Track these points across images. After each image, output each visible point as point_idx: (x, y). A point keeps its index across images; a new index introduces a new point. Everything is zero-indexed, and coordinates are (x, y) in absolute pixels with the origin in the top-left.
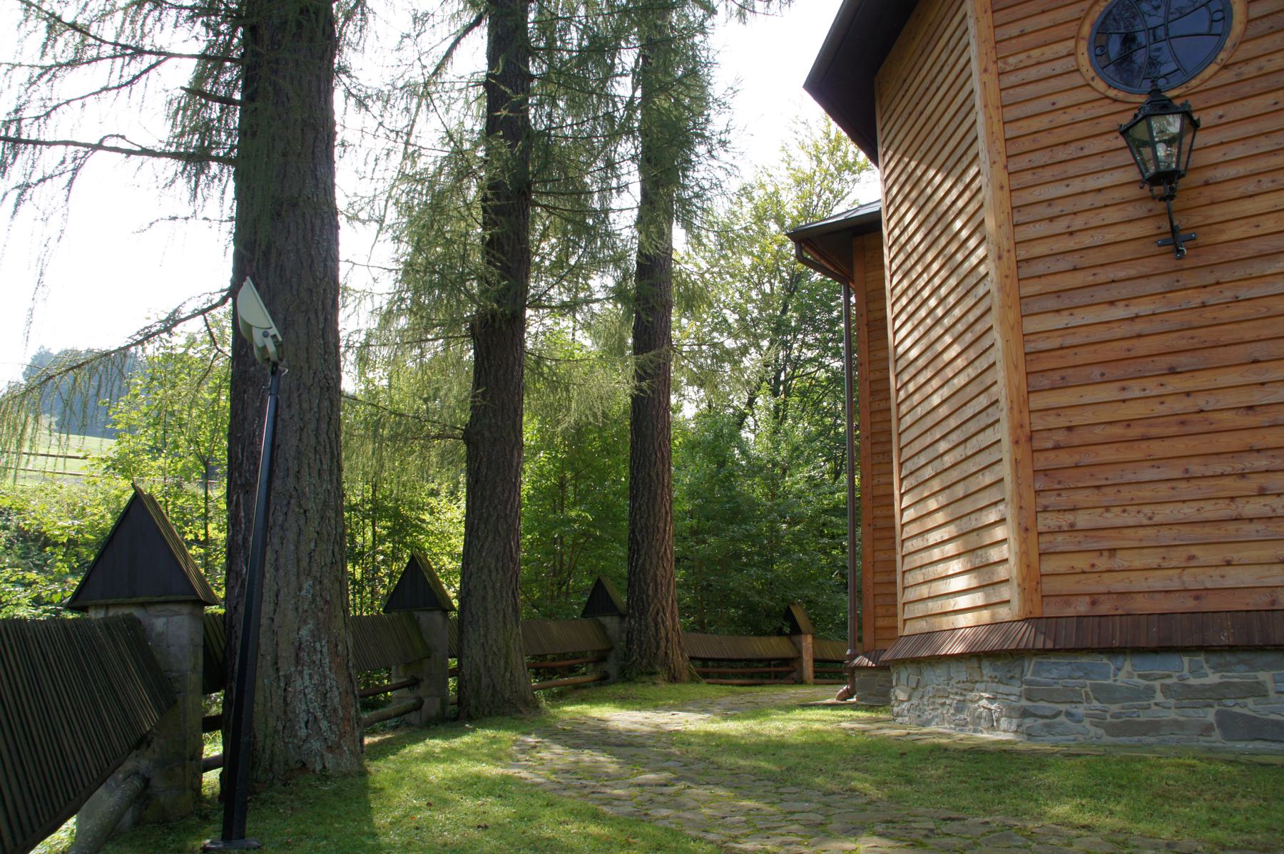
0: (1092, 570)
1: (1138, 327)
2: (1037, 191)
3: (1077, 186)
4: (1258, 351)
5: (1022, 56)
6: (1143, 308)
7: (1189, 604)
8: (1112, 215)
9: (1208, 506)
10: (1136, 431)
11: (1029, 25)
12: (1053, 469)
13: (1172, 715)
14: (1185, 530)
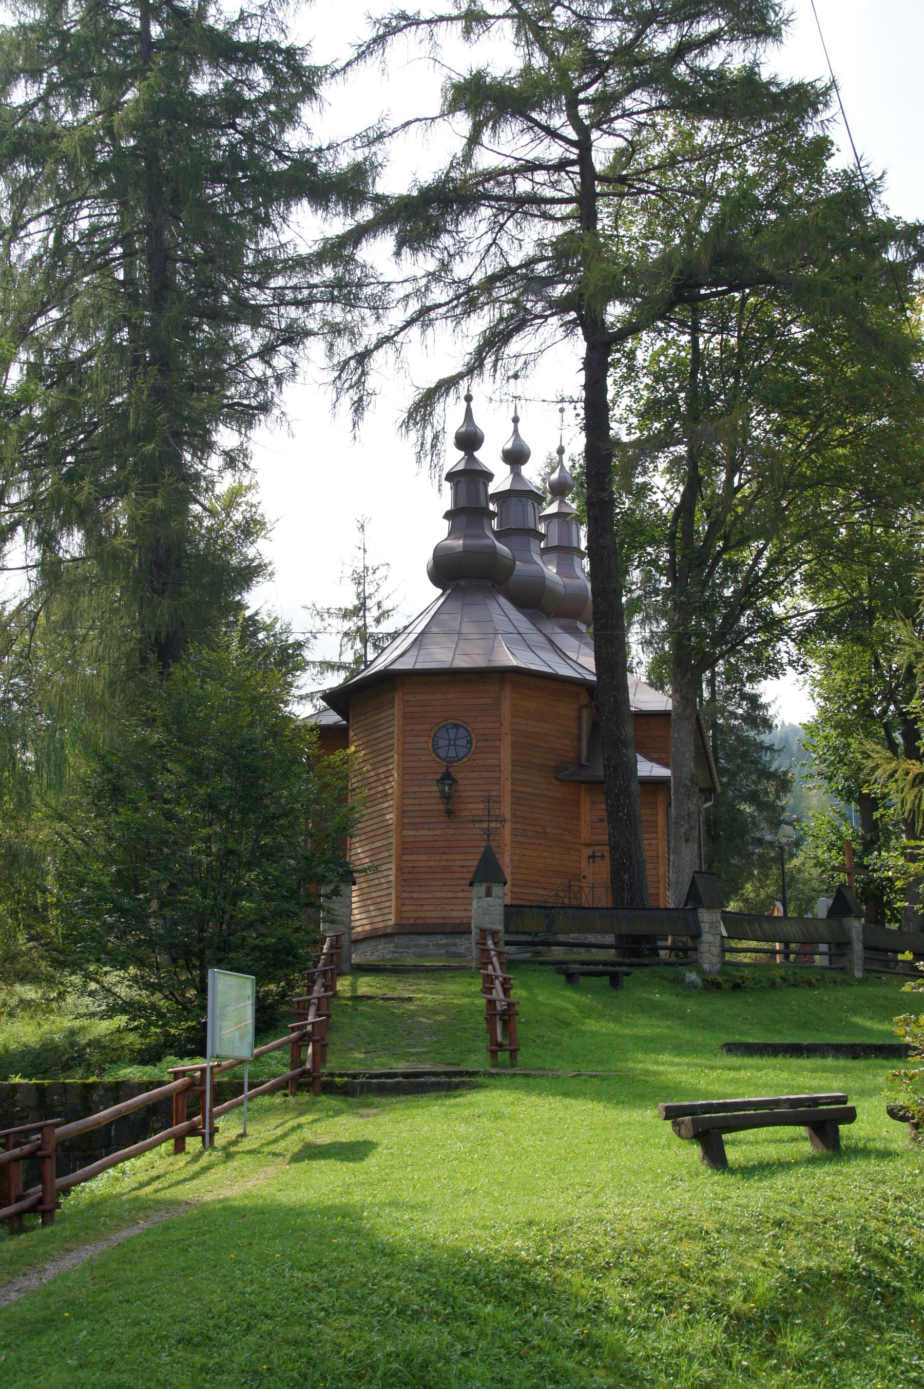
0: (416, 911)
3: (423, 789)
6: (437, 832)
7: (440, 921)
8: (432, 801)
12: (407, 878)
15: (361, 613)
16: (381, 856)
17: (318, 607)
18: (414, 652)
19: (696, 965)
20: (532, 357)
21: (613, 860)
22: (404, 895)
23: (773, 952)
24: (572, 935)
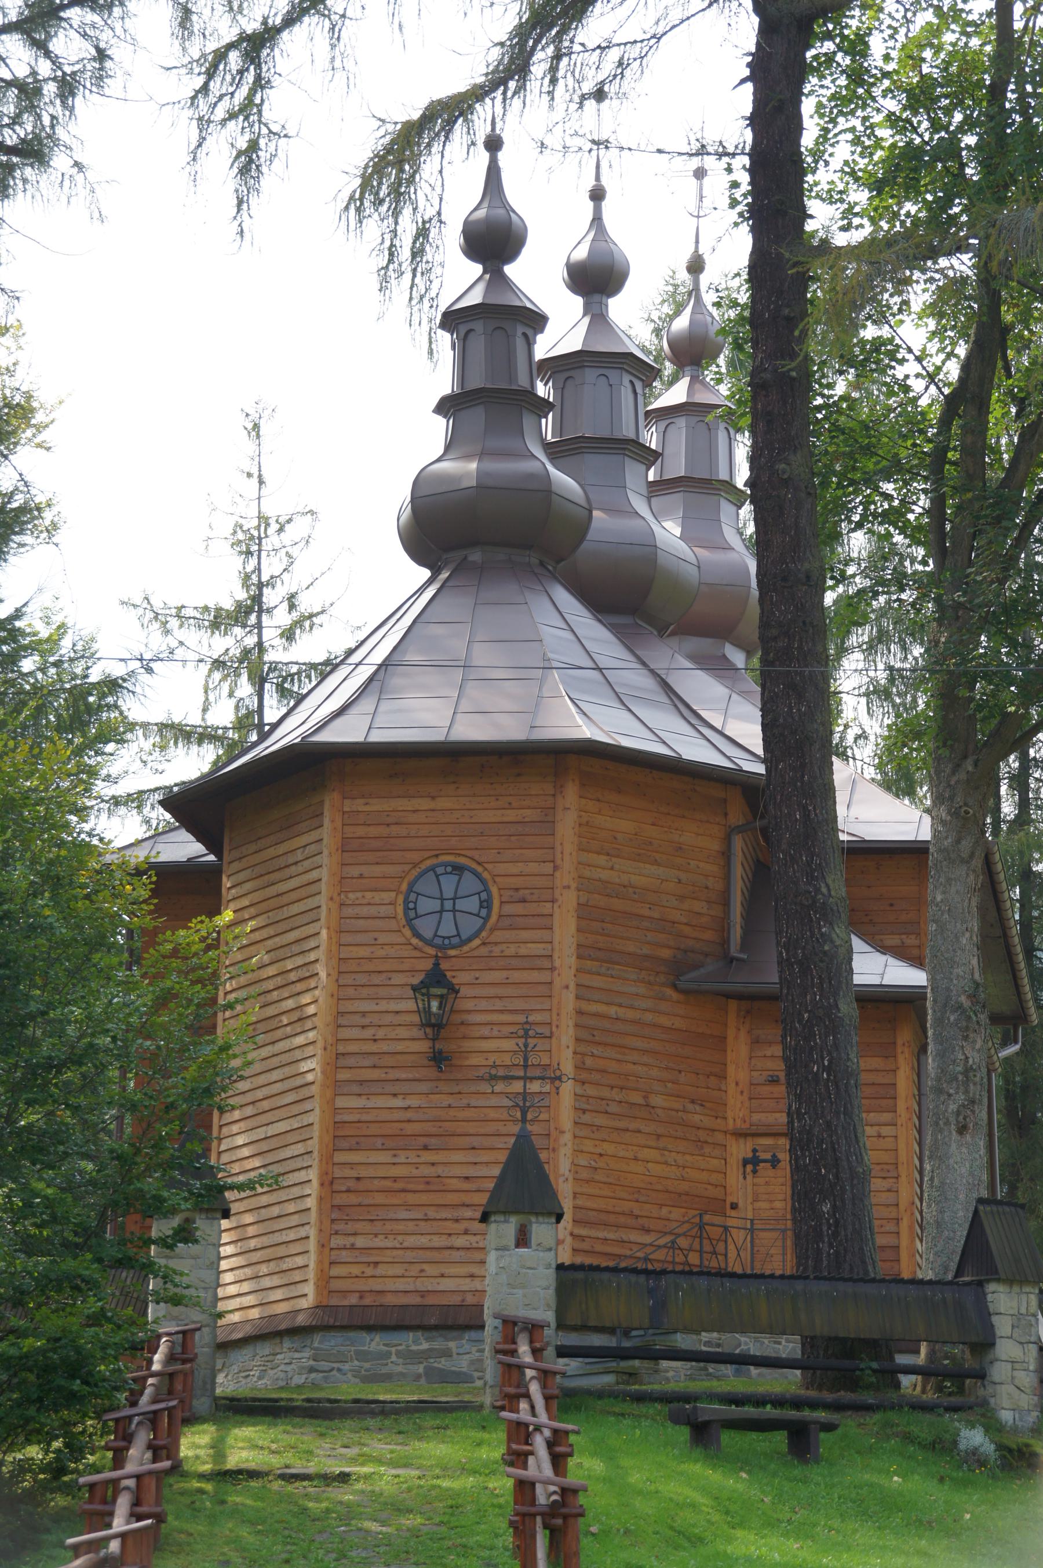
1: (409, 1115)
2: (357, 1003)
3: (383, 1006)
4: (476, 1141)
5: (359, 895)
6: (413, 1102)
7: (415, 1300)
8: (403, 1033)
9: (435, 1238)
10: (399, 1185)
11: (365, 870)
12: (344, 1203)
13: (400, 1369)
14: (421, 1252)
15: (253, 619)
16: (288, 1152)
17: (158, 605)
18: (367, 705)
19: (982, 1413)
20: (634, 51)
21: (797, 1168)
22: (337, 1241)
24: (705, 1336)
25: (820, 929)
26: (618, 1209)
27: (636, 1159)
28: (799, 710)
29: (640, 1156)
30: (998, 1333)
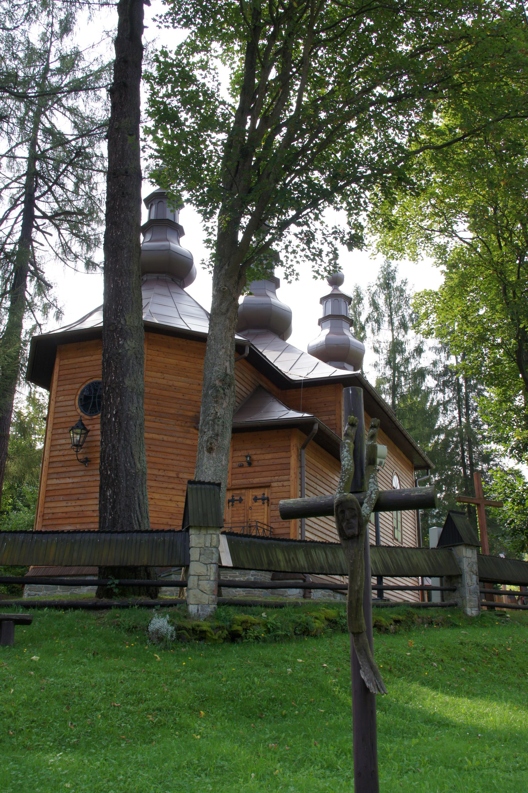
10: (68, 516)
23: (429, 589)
25: (119, 341)
26: (160, 522)
27: (171, 500)
28: (116, 234)
29: (173, 499)
30: (191, 559)
